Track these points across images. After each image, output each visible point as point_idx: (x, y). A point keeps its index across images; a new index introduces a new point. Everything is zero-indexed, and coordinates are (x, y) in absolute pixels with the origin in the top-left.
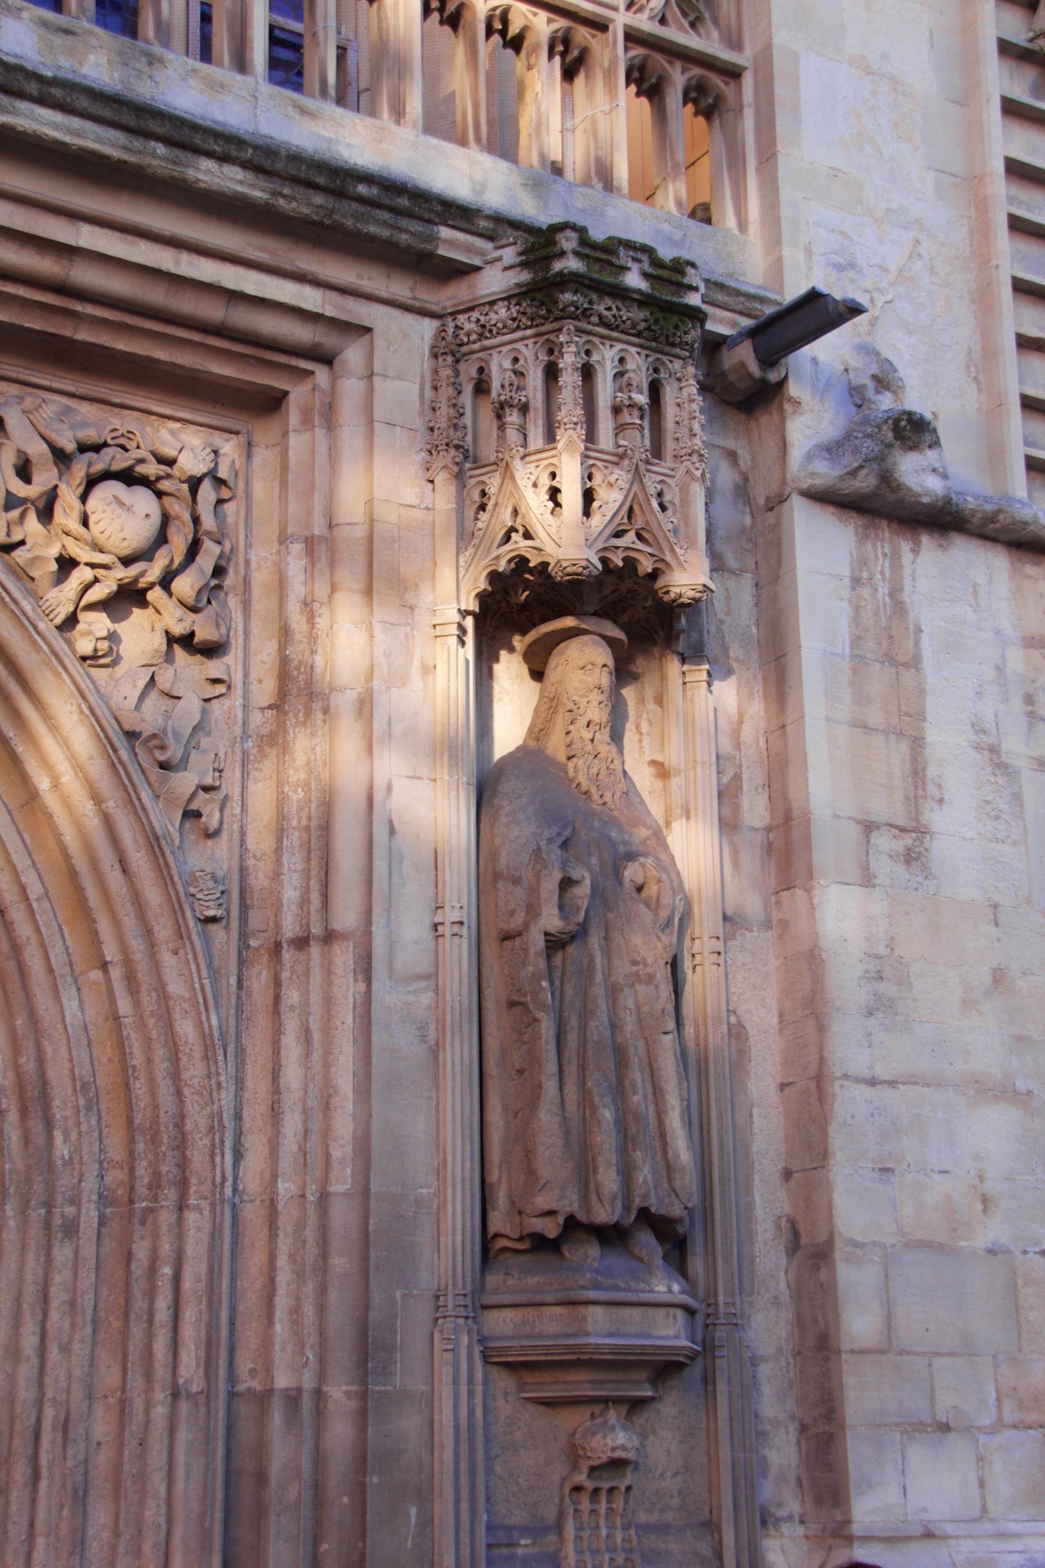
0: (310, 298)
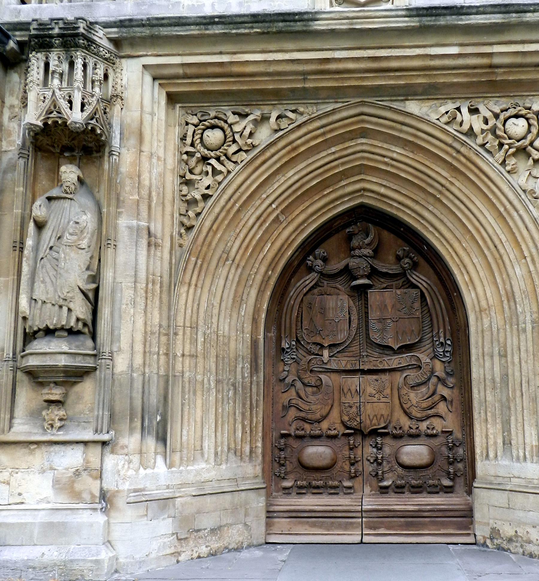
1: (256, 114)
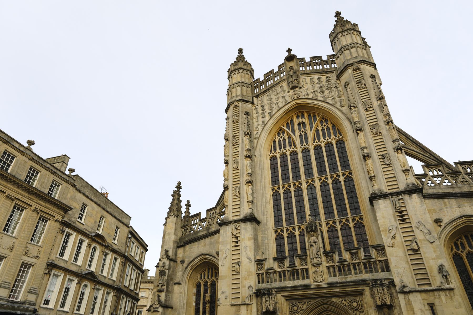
0: (360, 288)
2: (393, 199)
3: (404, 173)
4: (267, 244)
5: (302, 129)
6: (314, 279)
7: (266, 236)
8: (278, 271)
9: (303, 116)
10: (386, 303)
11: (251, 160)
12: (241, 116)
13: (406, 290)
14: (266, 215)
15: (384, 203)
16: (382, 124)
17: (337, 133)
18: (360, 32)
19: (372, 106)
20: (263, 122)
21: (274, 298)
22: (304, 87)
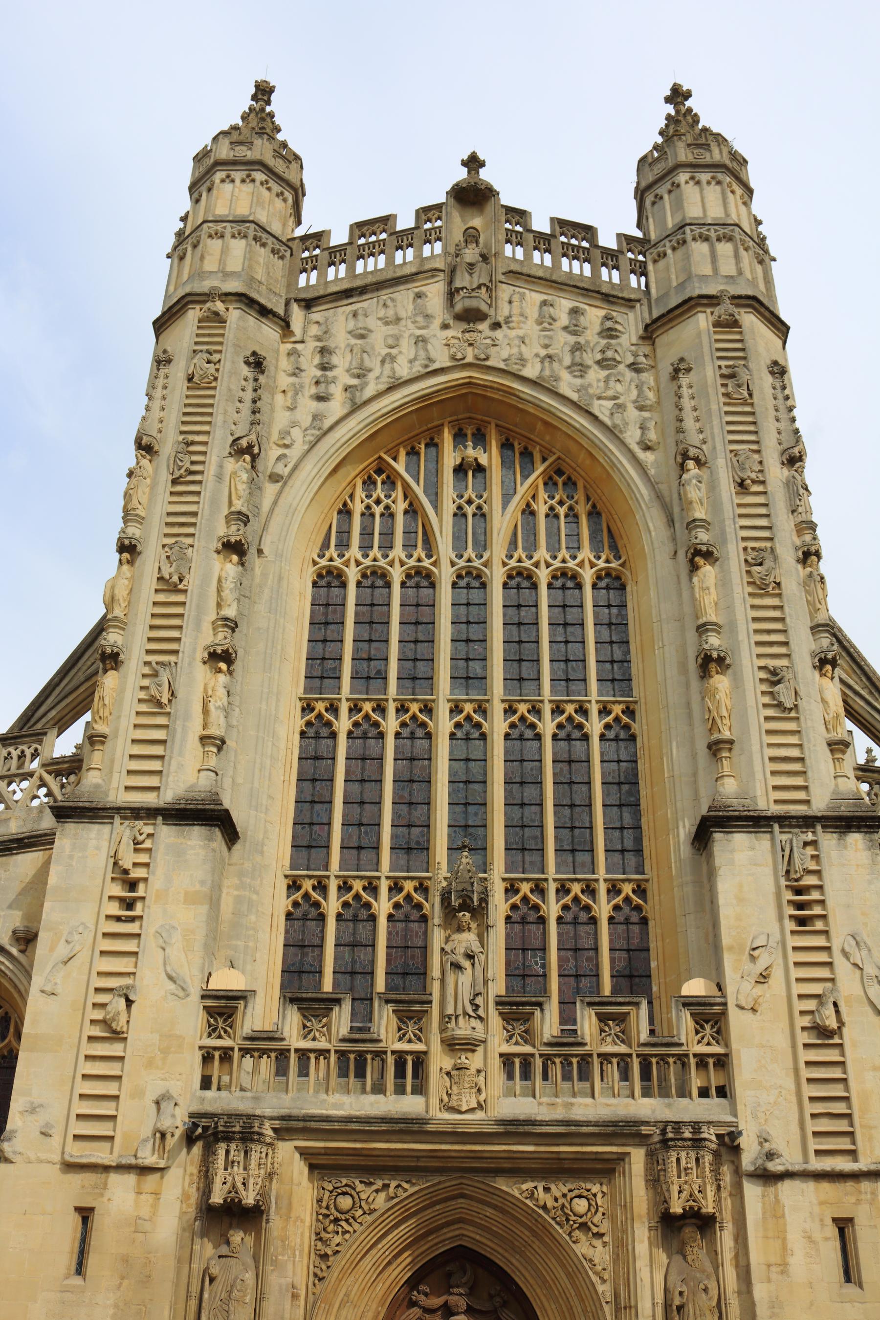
0: (614, 1149)
1: (379, 1183)
2: (784, 837)
3: (832, 751)
4: (251, 932)
5: (470, 493)
6: (446, 1098)
7: (254, 897)
8: (297, 1050)
9: (480, 439)
10: (700, 1208)
11: (243, 565)
12: (228, 365)
13: (775, 1166)
14: (267, 809)
15: (752, 848)
16: (787, 555)
17: (602, 541)
18: (750, 191)
19: (762, 479)
20: (315, 417)
21: (264, 1155)
22: (511, 325)
